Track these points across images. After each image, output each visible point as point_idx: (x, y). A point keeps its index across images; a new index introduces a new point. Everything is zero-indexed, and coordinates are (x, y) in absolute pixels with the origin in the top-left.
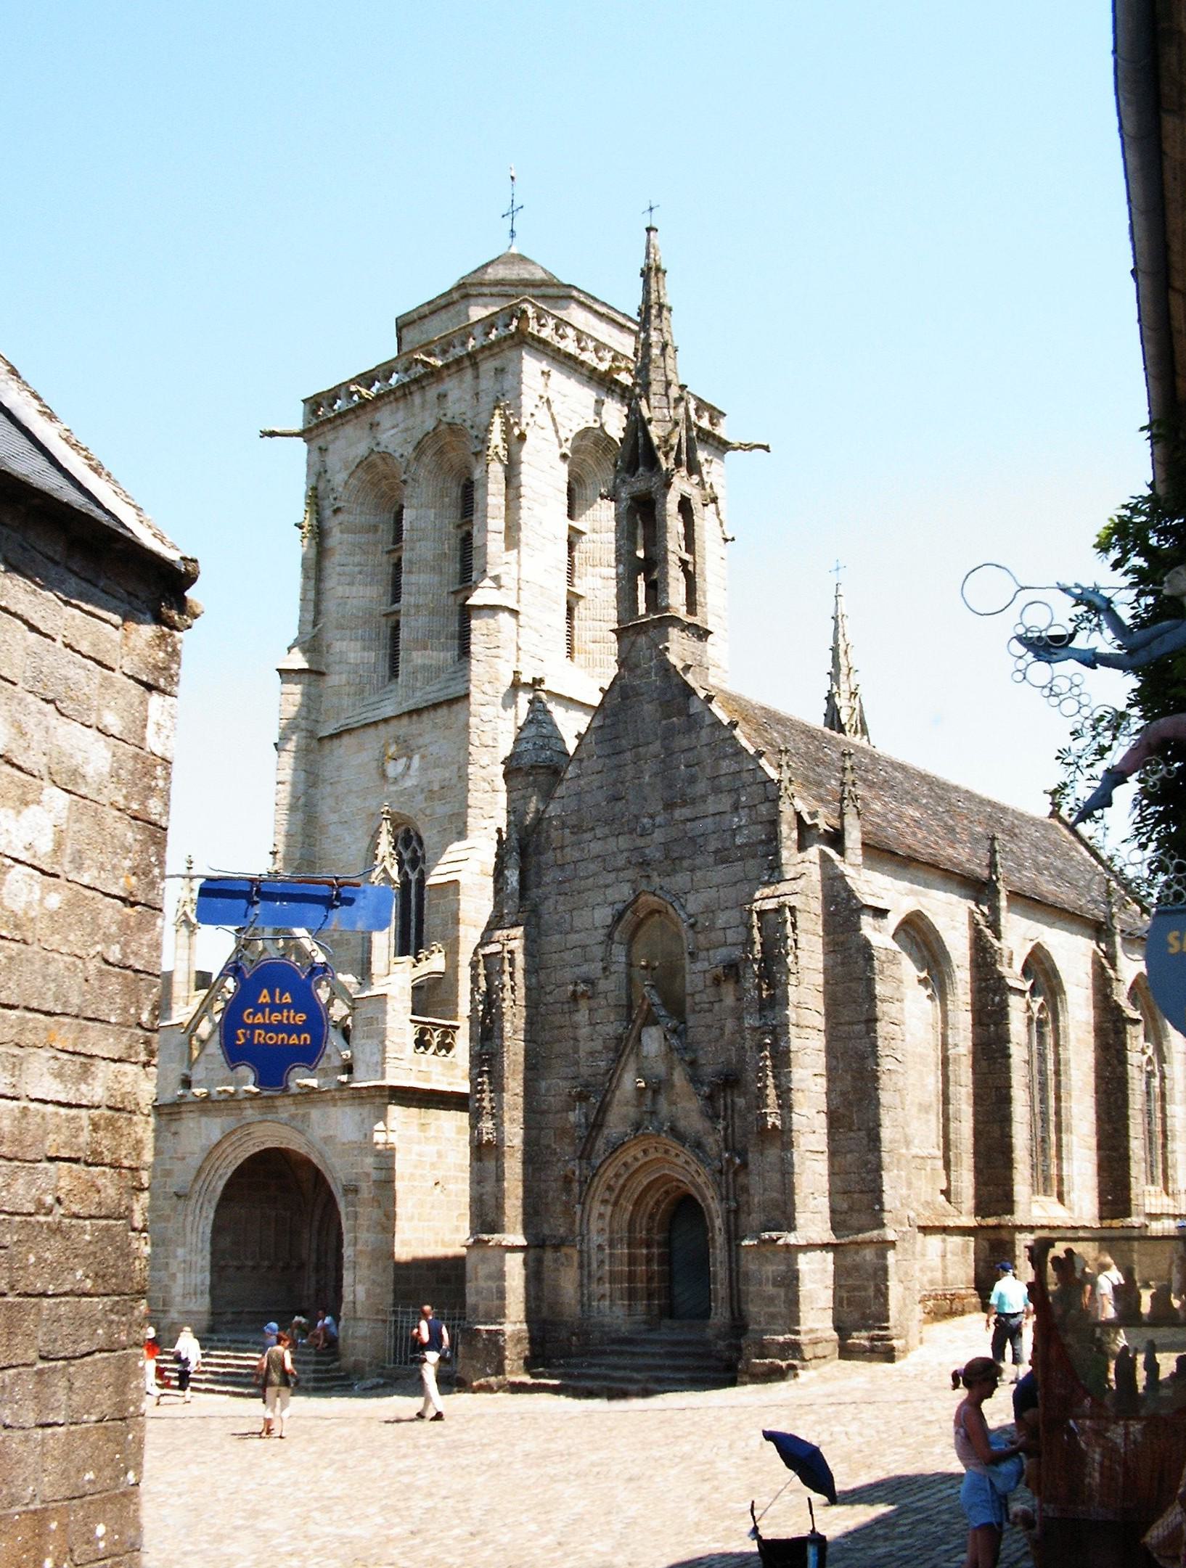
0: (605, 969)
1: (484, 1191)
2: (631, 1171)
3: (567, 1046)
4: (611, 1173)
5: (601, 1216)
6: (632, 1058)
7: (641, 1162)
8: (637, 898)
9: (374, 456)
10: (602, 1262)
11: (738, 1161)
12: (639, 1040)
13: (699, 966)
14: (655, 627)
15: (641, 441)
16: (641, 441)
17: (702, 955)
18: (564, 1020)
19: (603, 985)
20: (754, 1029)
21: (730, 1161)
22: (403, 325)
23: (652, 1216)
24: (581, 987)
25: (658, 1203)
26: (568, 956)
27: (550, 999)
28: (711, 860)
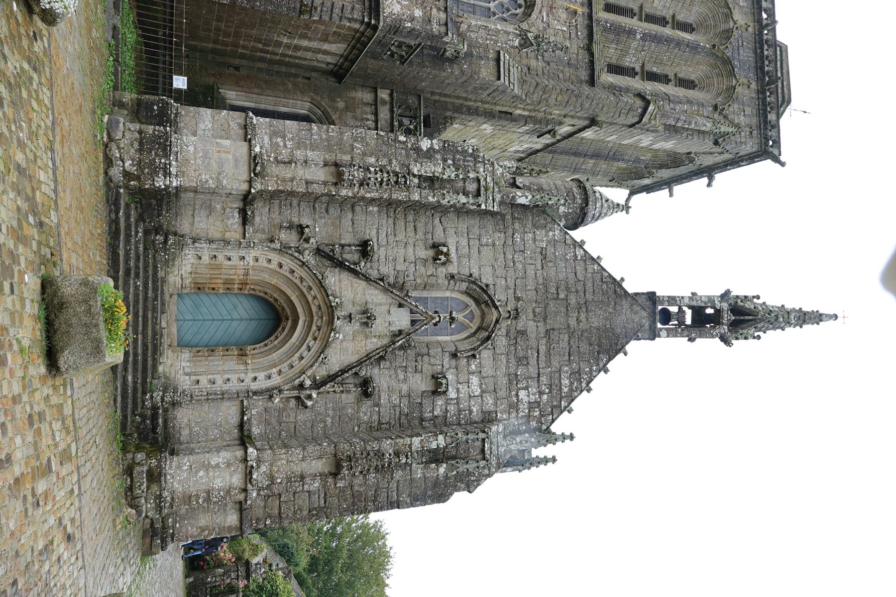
0: (452, 277)
1: (299, 164)
2: (306, 292)
3: (401, 237)
4: (304, 275)
5: (270, 261)
6: (390, 300)
7: (310, 299)
8: (496, 308)
9: (732, 24)
10: (230, 259)
11: (309, 403)
12: (400, 306)
13: (446, 360)
14: (650, 326)
15: (747, 318)
16: (747, 318)
17: (454, 362)
18: (420, 235)
19: (442, 271)
20: (410, 446)
21: (309, 397)
22: (783, 49)
23: (266, 293)
24: (443, 258)
25: (276, 300)
26: (464, 242)
27: (437, 221)
28: (512, 370)
